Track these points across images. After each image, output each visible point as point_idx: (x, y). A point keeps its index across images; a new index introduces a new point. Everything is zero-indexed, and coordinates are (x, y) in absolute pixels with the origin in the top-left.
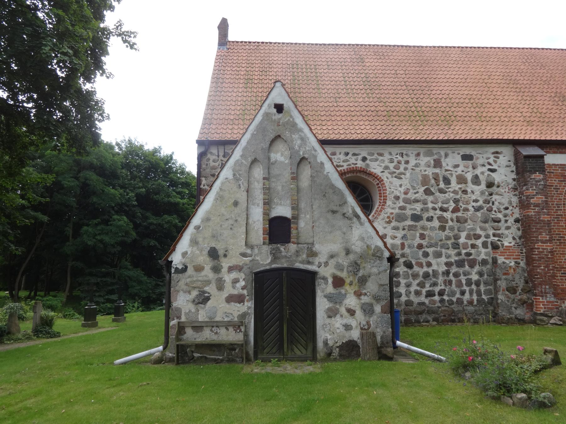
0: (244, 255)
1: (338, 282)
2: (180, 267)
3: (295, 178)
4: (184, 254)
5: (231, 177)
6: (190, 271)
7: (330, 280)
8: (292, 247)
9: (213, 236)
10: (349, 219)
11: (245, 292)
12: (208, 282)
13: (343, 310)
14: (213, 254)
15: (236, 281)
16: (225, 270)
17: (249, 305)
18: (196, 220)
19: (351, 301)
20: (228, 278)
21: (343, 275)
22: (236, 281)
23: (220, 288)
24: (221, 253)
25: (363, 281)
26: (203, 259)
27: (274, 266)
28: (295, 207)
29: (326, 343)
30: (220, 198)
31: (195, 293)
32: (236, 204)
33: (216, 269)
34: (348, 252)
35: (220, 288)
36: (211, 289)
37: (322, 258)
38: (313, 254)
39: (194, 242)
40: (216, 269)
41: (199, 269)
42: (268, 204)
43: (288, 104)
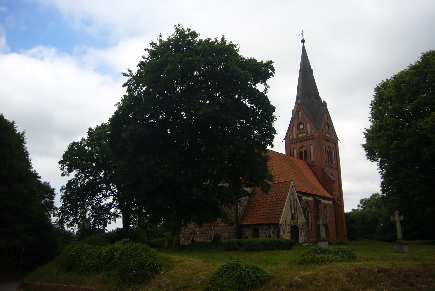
0: (289, 222)
1: (301, 229)
2: (281, 224)
3: (294, 204)
4: (281, 221)
5: (287, 203)
6: (282, 225)
7: (300, 229)
8: (295, 220)
9: (285, 217)
10: (302, 215)
11: (290, 231)
12: (285, 228)
13: (302, 236)
14: (285, 222)
15: (288, 228)
16: (287, 225)
17: (290, 234)
18: (283, 213)
19: (303, 234)
20: (288, 227)
21: (302, 227)
22: (288, 228)
23: (287, 230)
24: (286, 221)
25: (304, 229)
26: (284, 223)
27: (294, 225)
28: (294, 211)
29: (300, 243)
30: (286, 208)
31: (283, 231)
32: (288, 210)
33: (286, 225)
34: (302, 222)
35: (287, 230)
36: (285, 230)
37: (299, 224)
38: (298, 222)
39: (283, 219)
40: (286, 225)
41: (283, 225)
42: (291, 210)
43: (293, 186)
